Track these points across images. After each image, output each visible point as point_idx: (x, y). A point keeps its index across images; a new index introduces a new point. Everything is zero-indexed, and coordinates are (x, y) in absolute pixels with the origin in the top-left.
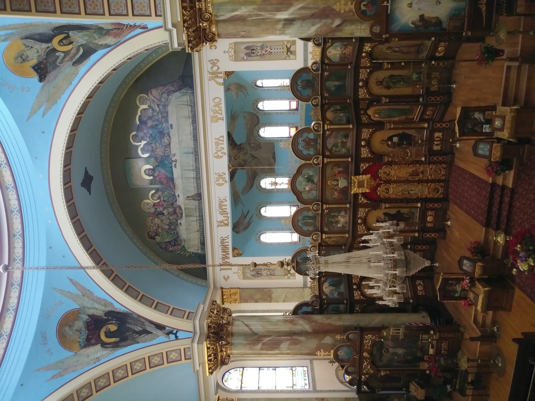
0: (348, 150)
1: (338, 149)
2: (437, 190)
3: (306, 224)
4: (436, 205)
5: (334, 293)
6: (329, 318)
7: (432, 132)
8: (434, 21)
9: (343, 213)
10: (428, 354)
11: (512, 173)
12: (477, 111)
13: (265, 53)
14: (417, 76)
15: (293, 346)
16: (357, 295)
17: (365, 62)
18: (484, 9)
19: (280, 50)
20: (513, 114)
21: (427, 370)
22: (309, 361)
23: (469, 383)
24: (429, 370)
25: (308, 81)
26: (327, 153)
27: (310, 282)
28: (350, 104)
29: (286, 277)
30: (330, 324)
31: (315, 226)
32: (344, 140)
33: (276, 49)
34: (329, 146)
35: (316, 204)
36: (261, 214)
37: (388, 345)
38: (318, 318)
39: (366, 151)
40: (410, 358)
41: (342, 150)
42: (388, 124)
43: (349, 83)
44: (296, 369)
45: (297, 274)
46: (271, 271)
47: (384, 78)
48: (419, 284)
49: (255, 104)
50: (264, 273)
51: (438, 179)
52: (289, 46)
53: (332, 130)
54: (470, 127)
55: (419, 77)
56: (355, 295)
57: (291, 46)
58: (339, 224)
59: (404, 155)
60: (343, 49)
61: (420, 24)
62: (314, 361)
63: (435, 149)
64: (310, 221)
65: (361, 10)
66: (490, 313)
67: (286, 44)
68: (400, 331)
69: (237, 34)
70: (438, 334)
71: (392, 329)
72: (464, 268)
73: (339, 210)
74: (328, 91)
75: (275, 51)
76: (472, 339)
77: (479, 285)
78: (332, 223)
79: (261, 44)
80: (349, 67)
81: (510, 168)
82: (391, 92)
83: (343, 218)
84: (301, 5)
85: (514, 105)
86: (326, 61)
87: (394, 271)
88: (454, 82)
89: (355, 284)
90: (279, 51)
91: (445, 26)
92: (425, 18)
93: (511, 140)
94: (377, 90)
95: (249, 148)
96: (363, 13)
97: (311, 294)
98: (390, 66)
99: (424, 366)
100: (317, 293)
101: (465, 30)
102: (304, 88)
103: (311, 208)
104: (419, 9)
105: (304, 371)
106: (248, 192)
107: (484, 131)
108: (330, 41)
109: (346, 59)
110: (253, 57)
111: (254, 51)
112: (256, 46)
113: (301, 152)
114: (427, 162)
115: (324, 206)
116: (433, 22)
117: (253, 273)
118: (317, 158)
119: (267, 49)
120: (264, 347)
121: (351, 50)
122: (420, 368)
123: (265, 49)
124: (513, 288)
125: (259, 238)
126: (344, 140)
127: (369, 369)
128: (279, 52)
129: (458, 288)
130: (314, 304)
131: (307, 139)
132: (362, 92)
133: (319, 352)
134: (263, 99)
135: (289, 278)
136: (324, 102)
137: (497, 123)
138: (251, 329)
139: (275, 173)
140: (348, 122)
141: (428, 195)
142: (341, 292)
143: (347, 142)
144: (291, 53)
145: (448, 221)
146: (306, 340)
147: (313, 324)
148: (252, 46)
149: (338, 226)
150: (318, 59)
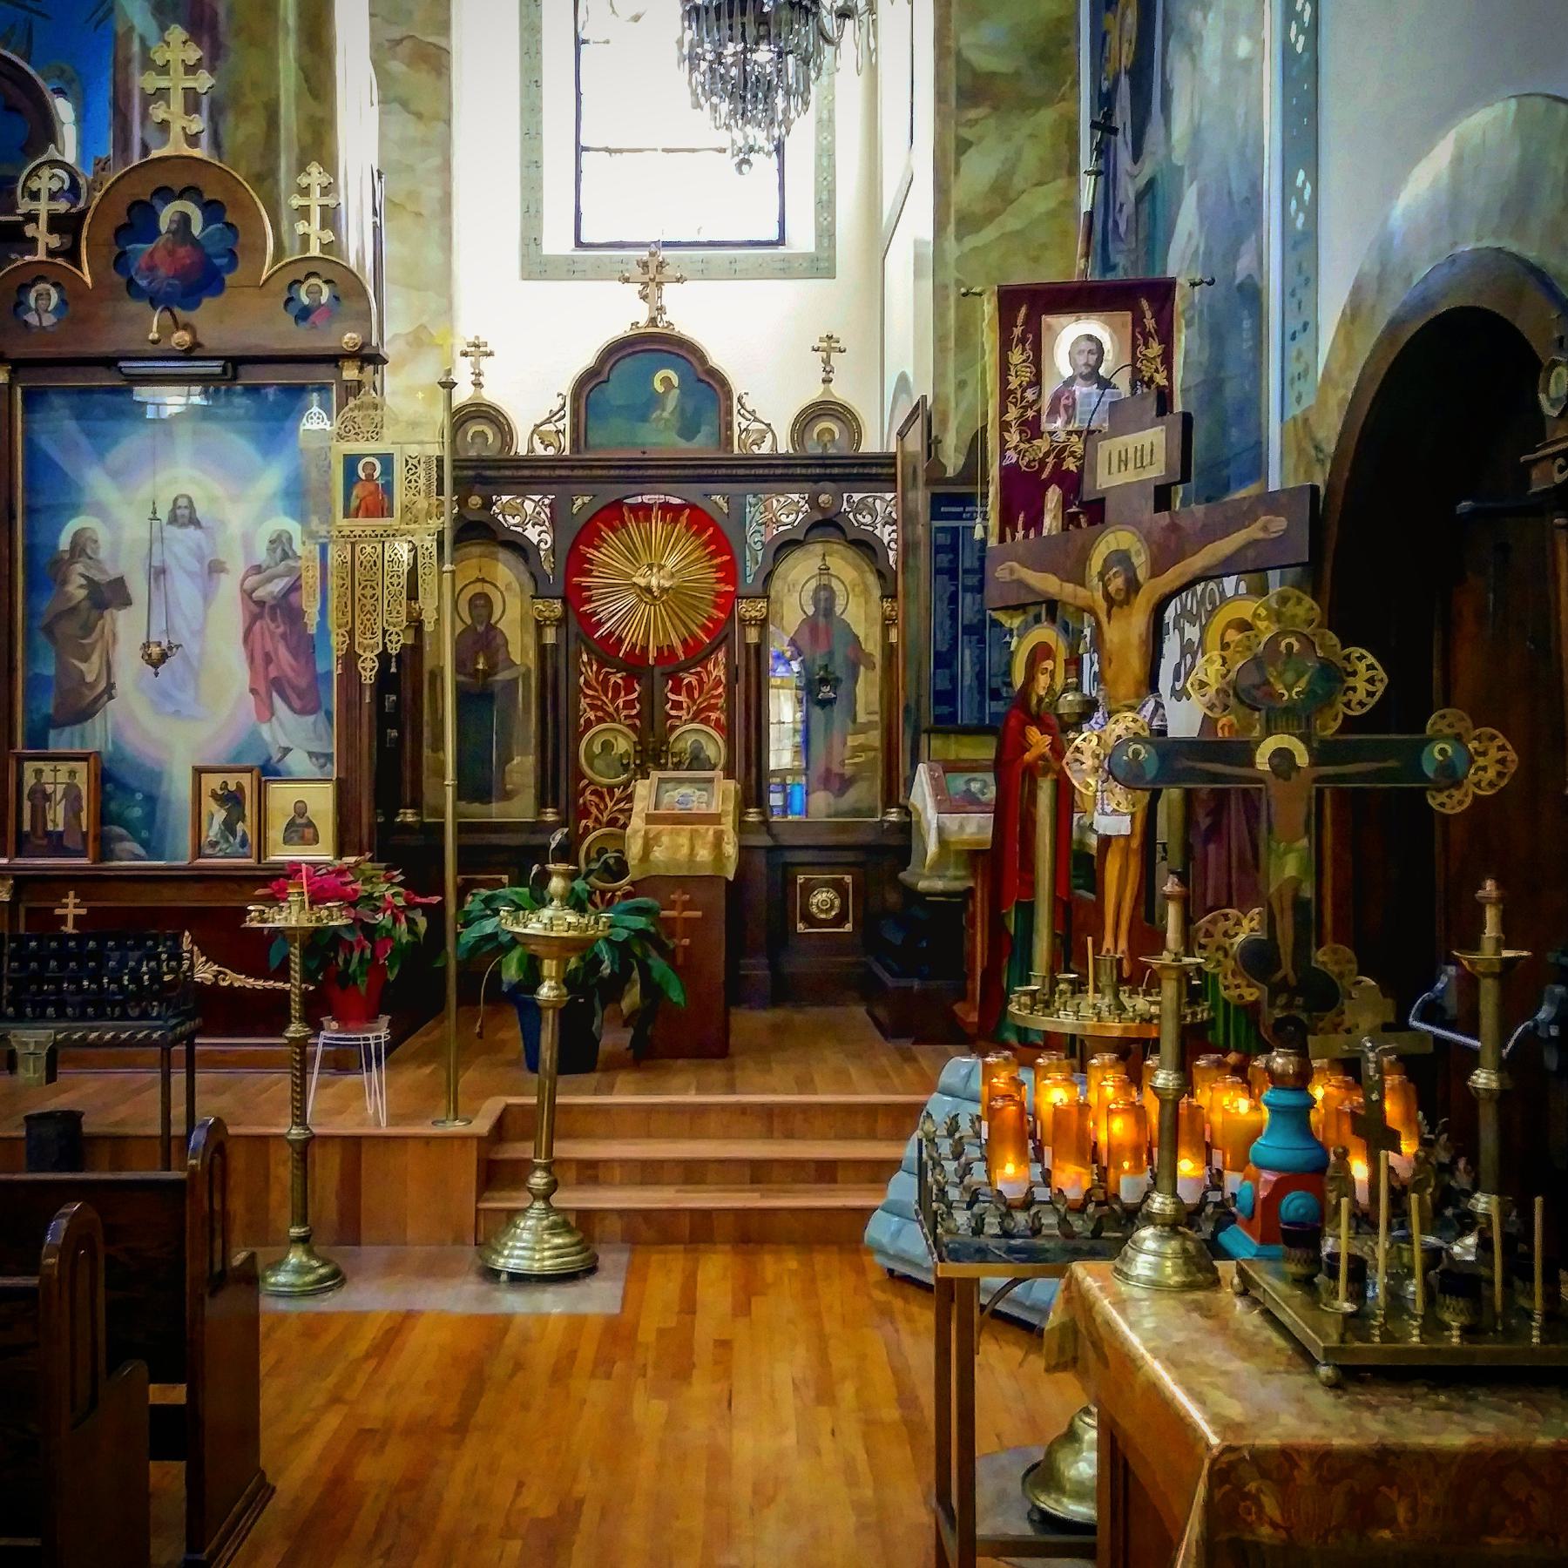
8: (91, 670)
61: (76, 590)
65: (157, 203)
92: (107, 613)
101: (20, 861)
116: (83, 666)
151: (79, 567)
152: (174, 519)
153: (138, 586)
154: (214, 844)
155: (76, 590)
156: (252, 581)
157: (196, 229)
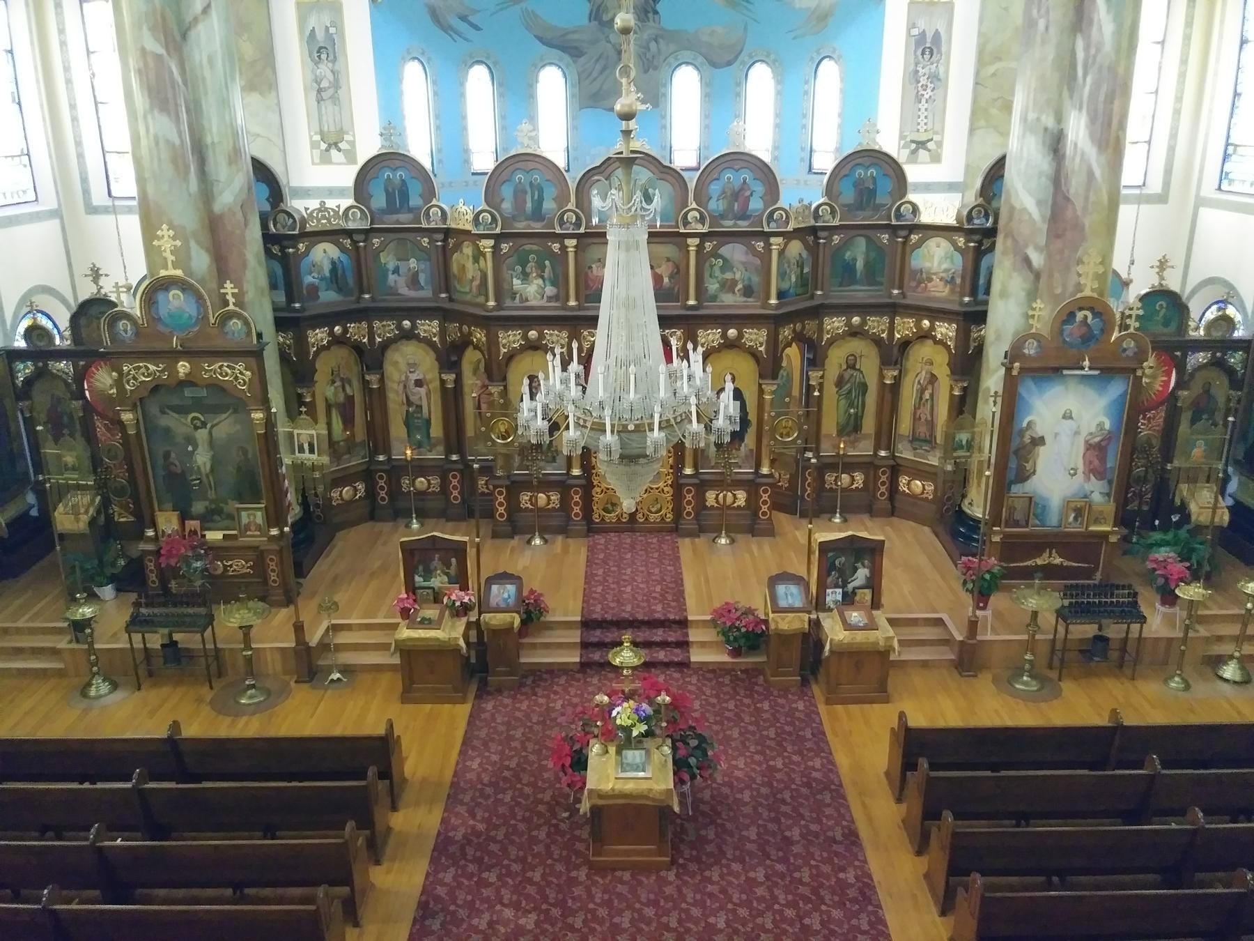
0: (714, 298)
1: (717, 273)
2: (609, 506)
3: (519, 194)
4: (577, 509)
5: (316, 276)
6: (259, 262)
7: (752, 486)
8: (1028, 466)
9: (550, 290)
10: (203, 529)
11: (725, 658)
12: (871, 572)
13: (920, 85)
14: (964, 442)
15: (165, 155)
16: (318, 336)
17: (905, 327)
18: (1039, 562)
19: (922, 124)
20: (882, 643)
21: (156, 531)
22: (55, 206)
23: (170, 636)
24: (156, 535)
25: (872, 193)
26: (708, 246)
27: (338, 207)
28: (812, 297)
29: (318, 138)
30: (244, 265)
31: (514, 218)
32: (740, 286)
33: (926, 114)
34: (725, 250)
35: (578, 218)
36: (471, 66)
37: (216, 425)
38: (254, 233)
39: (713, 341)
40: (195, 485)
41: (715, 280)
42: (775, 387)
43: (860, 293)
44: (25, 166)
45: (355, 169)
46: (331, 91)
47: (862, 372)
48: (356, 490)
49: (768, 55)
50: (324, 69)
51: (595, 508)
52: (930, 145)
53: (766, 256)
54: (837, 563)
55: (961, 447)
56: (317, 331)
57: (929, 151)
58: (519, 282)
59: (785, 427)
60: (943, 275)
61: (1027, 440)
62: (55, 224)
63: (707, 494)
64: (529, 205)
66: (396, 660)
67: (936, 138)
68: (307, 455)
69: (1043, 11)
70: (275, 547)
71: (313, 432)
72: (495, 588)
73: (559, 281)
74: (845, 244)
75: (923, 110)
76: (299, 628)
77: (461, 625)
78: (524, 264)
79: (942, 75)
80: (896, 292)
81: (736, 653)
82: (830, 390)
83: (537, 292)
84: (1098, 173)
85: (899, 641)
86: (914, 238)
87: (613, 426)
88: (845, 520)
89: (345, 331)
90: (922, 120)
91: (1016, 489)
93: (827, 648)
94: (836, 358)
95: (645, 36)
96: (1072, 315)
97: (306, 209)
98: (888, 382)
99: (168, 522)
100: (312, 226)
102: (858, 184)
103: (570, 206)
104: (1056, 435)
105: (24, 192)
106: (528, 28)
107: (829, 591)
108: (972, 244)
109: (913, 284)
110: (915, 52)
111: (927, 56)
112: (938, 62)
113: (715, 176)
114: (682, 481)
115: (570, 243)
117: (320, 35)
118: (702, 220)
119: (929, 90)
120: (151, 64)
121: (938, 294)
122: (158, 513)
123: (929, 84)
124: (463, 701)
125: (414, 58)
126: (740, 286)
127: (134, 378)
128: (919, 120)
129: (439, 581)
130: (281, 217)
131: (748, 193)
132: (836, 324)
133: (171, 233)
134: (779, 79)
135: (314, 145)
136: (821, 234)
137: (855, 614)
138: (196, 20)
139: (581, 109)
140: (781, 295)
141: (599, 490)
142: (320, 294)
143: (734, 293)
144: (914, 152)
145: (542, 538)
146: (190, 195)
147: (240, 215)
148: (939, 52)
149: (514, 280)
150: (926, 218)
151: (1028, 433)
152: (1064, 417)
153: (1048, 439)
154: (1070, 524)
155: (1027, 440)
156: (1089, 437)
157: (1089, 320)
